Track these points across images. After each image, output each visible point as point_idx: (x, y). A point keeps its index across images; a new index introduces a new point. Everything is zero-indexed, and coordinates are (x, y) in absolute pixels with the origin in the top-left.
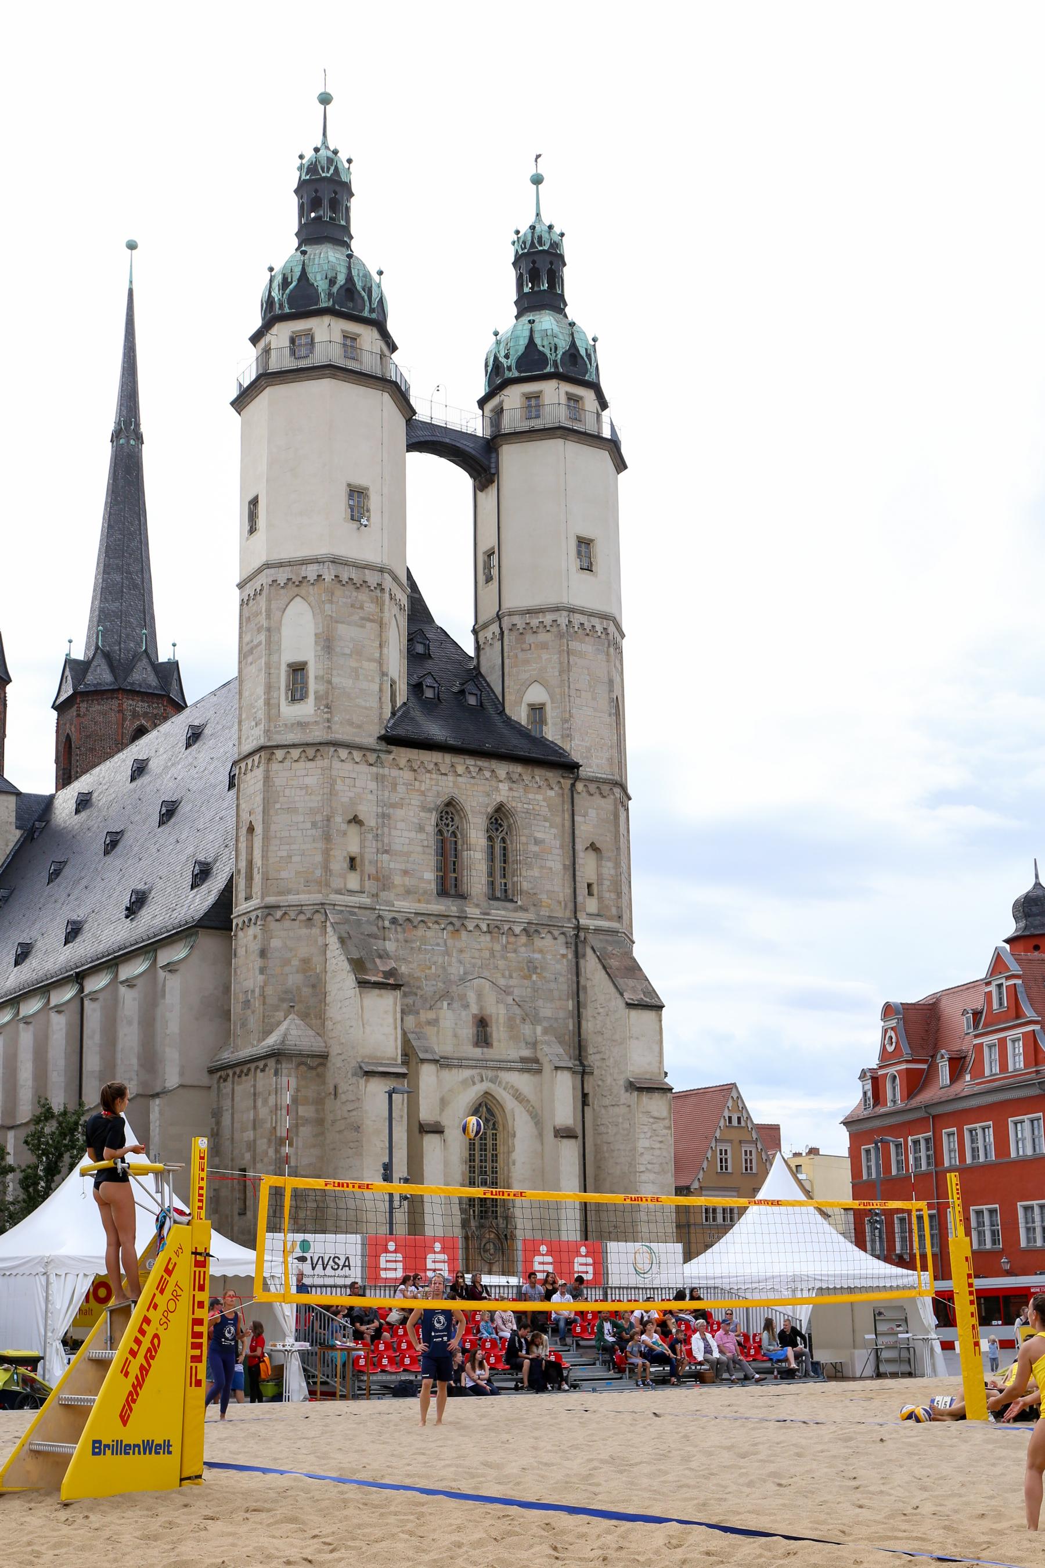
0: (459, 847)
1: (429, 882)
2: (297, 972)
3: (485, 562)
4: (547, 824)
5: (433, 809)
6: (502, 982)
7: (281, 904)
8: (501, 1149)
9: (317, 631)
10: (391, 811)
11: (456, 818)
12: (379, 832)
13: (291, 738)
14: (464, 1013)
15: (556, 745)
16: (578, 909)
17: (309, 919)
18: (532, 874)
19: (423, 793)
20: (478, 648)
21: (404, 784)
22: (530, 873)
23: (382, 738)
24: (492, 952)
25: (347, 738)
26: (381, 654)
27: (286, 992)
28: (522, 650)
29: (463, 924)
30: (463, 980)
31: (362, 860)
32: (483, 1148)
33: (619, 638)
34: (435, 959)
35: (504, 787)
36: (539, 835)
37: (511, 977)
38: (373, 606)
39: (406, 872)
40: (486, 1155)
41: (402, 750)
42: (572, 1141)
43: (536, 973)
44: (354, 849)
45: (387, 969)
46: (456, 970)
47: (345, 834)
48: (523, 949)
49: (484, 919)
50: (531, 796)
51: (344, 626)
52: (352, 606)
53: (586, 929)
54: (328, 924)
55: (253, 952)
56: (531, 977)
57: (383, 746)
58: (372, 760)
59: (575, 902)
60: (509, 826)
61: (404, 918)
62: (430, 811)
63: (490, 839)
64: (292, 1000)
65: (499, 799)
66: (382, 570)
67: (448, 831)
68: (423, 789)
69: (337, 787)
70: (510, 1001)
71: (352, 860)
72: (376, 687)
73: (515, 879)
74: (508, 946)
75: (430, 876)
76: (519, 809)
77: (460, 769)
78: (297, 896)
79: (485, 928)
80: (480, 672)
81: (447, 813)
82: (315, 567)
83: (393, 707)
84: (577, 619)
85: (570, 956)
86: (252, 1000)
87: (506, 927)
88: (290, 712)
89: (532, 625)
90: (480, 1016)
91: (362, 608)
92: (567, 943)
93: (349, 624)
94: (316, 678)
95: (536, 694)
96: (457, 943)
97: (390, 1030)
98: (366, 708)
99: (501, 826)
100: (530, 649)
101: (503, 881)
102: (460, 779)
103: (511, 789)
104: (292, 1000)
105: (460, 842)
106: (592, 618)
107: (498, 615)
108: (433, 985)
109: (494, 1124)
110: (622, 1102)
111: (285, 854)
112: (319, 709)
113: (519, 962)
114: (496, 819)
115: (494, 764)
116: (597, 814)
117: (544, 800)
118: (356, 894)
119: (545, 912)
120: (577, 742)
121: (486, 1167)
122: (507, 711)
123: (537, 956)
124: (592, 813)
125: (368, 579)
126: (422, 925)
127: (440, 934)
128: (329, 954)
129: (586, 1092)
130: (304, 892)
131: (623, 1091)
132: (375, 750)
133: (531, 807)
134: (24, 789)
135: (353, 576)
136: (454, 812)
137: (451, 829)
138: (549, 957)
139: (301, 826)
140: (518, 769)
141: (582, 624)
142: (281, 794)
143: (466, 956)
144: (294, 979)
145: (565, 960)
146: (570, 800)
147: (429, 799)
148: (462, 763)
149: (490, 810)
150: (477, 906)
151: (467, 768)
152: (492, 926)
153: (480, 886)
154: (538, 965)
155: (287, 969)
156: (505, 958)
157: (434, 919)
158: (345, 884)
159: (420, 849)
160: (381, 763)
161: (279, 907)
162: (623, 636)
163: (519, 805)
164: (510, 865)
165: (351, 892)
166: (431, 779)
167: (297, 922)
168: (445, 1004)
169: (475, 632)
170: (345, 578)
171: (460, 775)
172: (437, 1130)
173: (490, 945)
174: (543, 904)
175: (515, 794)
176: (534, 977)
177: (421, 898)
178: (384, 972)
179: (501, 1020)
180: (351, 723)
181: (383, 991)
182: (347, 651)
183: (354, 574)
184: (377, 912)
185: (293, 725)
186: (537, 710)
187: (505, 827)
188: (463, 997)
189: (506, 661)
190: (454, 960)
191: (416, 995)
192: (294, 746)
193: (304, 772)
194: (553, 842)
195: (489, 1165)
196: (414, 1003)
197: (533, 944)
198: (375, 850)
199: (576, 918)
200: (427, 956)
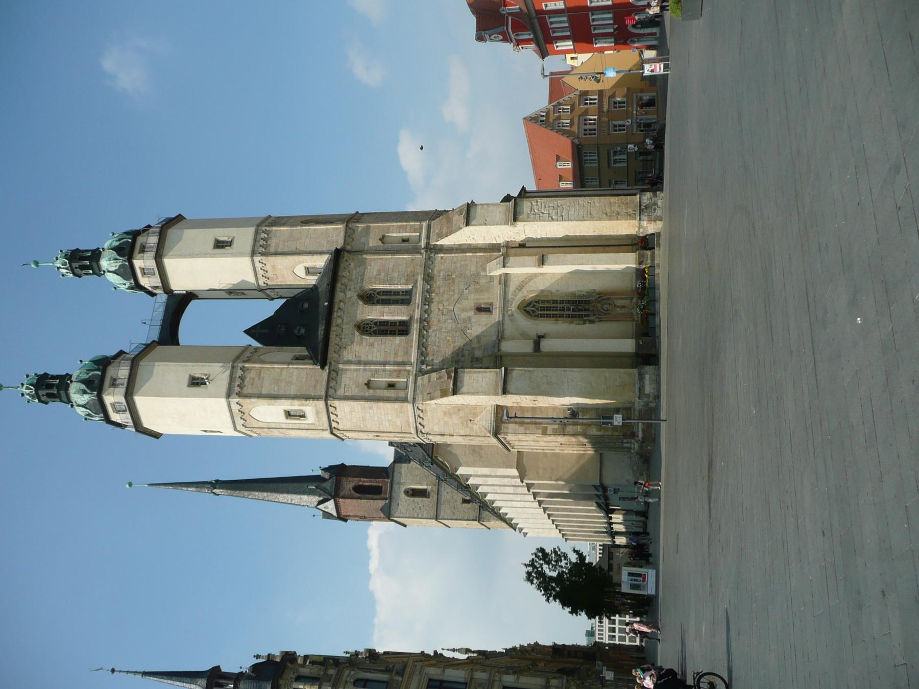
3: (234, 295)
5: (361, 337)
6: (456, 296)
7: (415, 426)
8: (550, 298)
14: (473, 320)
15: (326, 261)
17: (422, 412)
20: (281, 298)
23: (323, 367)
28: (277, 278)
30: (455, 320)
32: (549, 309)
33: (271, 219)
34: (443, 337)
36: (375, 272)
37: (454, 290)
39: (396, 354)
40: (553, 307)
41: (329, 356)
42: (544, 257)
43: (451, 276)
45: (446, 376)
46: (449, 325)
49: (421, 307)
50: (354, 278)
53: (428, 244)
56: (453, 278)
57: (327, 368)
62: (362, 339)
65: (356, 297)
67: (374, 327)
70: (466, 292)
72: (295, 370)
75: (397, 340)
78: (410, 418)
80: (294, 297)
88: (311, 418)
90: (475, 310)
91: (253, 379)
94: (292, 405)
95: (300, 271)
96: (435, 324)
97: (480, 375)
98: (307, 378)
99: (371, 294)
102: (345, 321)
104: (467, 422)
106: (257, 240)
107: (260, 291)
108: (458, 338)
109: (536, 302)
110: (523, 228)
113: (445, 285)
114: (367, 297)
115: (336, 300)
116: (364, 237)
121: (560, 307)
123: (442, 274)
129: (518, 245)
131: (515, 228)
132: (329, 373)
133: (359, 277)
134: (392, 460)
136: (363, 323)
137: (373, 325)
140: (339, 285)
144: (455, 419)
148: (336, 320)
150: (414, 311)
151: (339, 317)
154: (447, 274)
157: (421, 338)
159: (383, 346)
161: (416, 427)
162: (270, 216)
163: (359, 284)
166: (345, 339)
167: (424, 418)
168: (468, 331)
169: (272, 299)
171: (343, 321)
172: (538, 341)
175: (353, 287)
176: (454, 276)
178: (448, 378)
179: (477, 297)
181: (458, 380)
184: (417, 373)
185: (318, 418)
186: (308, 271)
187: (372, 292)
188: (465, 321)
191: (463, 349)
192: (329, 418)
193: (343, 412)
195: (559, 305)
196: (468, 350)
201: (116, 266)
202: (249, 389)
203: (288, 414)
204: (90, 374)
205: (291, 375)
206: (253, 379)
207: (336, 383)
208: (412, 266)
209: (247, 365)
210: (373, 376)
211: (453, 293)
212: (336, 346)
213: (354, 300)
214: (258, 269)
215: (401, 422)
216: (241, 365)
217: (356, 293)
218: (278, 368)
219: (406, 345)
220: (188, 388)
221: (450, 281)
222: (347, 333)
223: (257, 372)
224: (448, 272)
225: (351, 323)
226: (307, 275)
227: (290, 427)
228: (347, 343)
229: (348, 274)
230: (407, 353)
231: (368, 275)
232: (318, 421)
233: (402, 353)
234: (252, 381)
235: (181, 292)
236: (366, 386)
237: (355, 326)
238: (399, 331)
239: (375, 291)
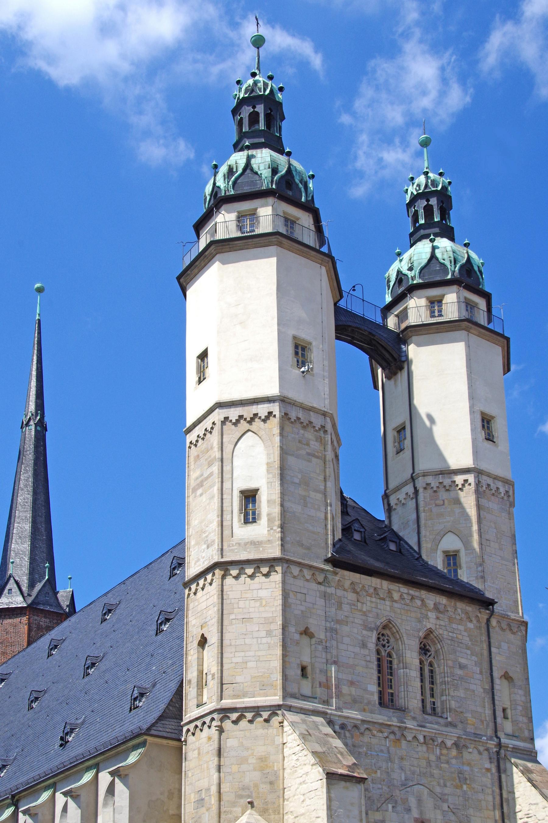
0: (395, 666)
1: (372, 694)
2: (255, 770)
4: (469, 652)
5: (374, 629)
9: (269, 461)
10: (338, 626)
11: (392, 640)
12: (328, 645)
15: (471, 585)
16: (498, 729)
18: (458, 695)
19: (365, 614)
21: (348, 604)
22: (456, 693)
23: (328, 561)
24: (429, 762)
26: (325, 487)
27: (244, 788)
29: (403, 734)
31: (313, 669)
35: (432, 615)
36: (463, 661)
38: (317, 444)
39: (352, 683)
41: (346, 573)
43: (466, 784)
44: (306, 659)
47: (297, 643)
48: (454, 761)
50: (454, 626)
52: (300, 442)
54: (286, 723)
55: (208, 752)
58: (320, 578)
59: (495, 723)
60: (436, 652)
61: (352, 725)
62: (371, 630)
63: (421, 662)
64: (249, 796)
66: (324, 414)
68: (364, 610)
69: (290, 600)
71: (303, 669)
72: (322, 516)
73: (444, 698)
74: (442, 757)
75: (374, 688)
76: (445, 637)
77: (396, 596)
79: (421, 739)
81: (383, 635)
83: (334, 539)
85: (494, 770)
86: (207, 798)
87: (440, 740)
89: (445, 484)
91: (308, 445)
92: (490, 758)
93: (298, 457)
94: (268, 501)
99: (429, 651)
100: (443, 505)
101: (433, 700)
102: (396, 605)
103: (438, 618)
105: (395, 662)
113: (452, 773)
114: (424, 645)
115: (424, 594)
117: (465, 630)
118: (310, 699)
119: (470, 729)
120: (489, 584)
122: (424, 557)
123: (466, 768)
125: (313, 420)
126: (367, 732)
127: (383, 742)
128: (287, 752)
130: (260, 695)
133: (455, 635)
135: (300, 416)
138: (476, 770)
139: (256, 635)
140: (443, 600)
143: (406, 763)
145: (489, 774)
146: (486, 633)
147: (370, 619)
149: (422, 634)
150: (414, 718)
152: (428, 738)
153: (416, 701)
154: (467, 777)
155: (244, 767)
156: (440, 768)
158: (299, 689)
159: (364, 663)
160: (329, 583)
163: (445, 633)
164: (439, 685)
165: (305, 698)
166: (371, 602)
170: (293, 415)
171: (396, 601)
173: (426, 755)
174: (469, 722)
175: (442, 623)
176: (465, 787)
177: (366, 707)
182: (297, 481)
185: (246, 544)
187: (433, 653)
189: (422, 515)
190: (396, 766)
197: (462, 757)
198: (325, 661)
199: (497, 737)
200: (373, 761)
211: (442, 784)
215: (242, 683)
217: (434, 628)
219: (365, 701)
220: (291, 335)
221: (457, 781)
222: (379, 607)
224: (470, 778)
227: (225, 496)
228: (365, 605)
230: (354, 703)
231: (459, 649)
232: (239, 544)
233: (353, 693)
236: (303, 629)
237: (390, 621)
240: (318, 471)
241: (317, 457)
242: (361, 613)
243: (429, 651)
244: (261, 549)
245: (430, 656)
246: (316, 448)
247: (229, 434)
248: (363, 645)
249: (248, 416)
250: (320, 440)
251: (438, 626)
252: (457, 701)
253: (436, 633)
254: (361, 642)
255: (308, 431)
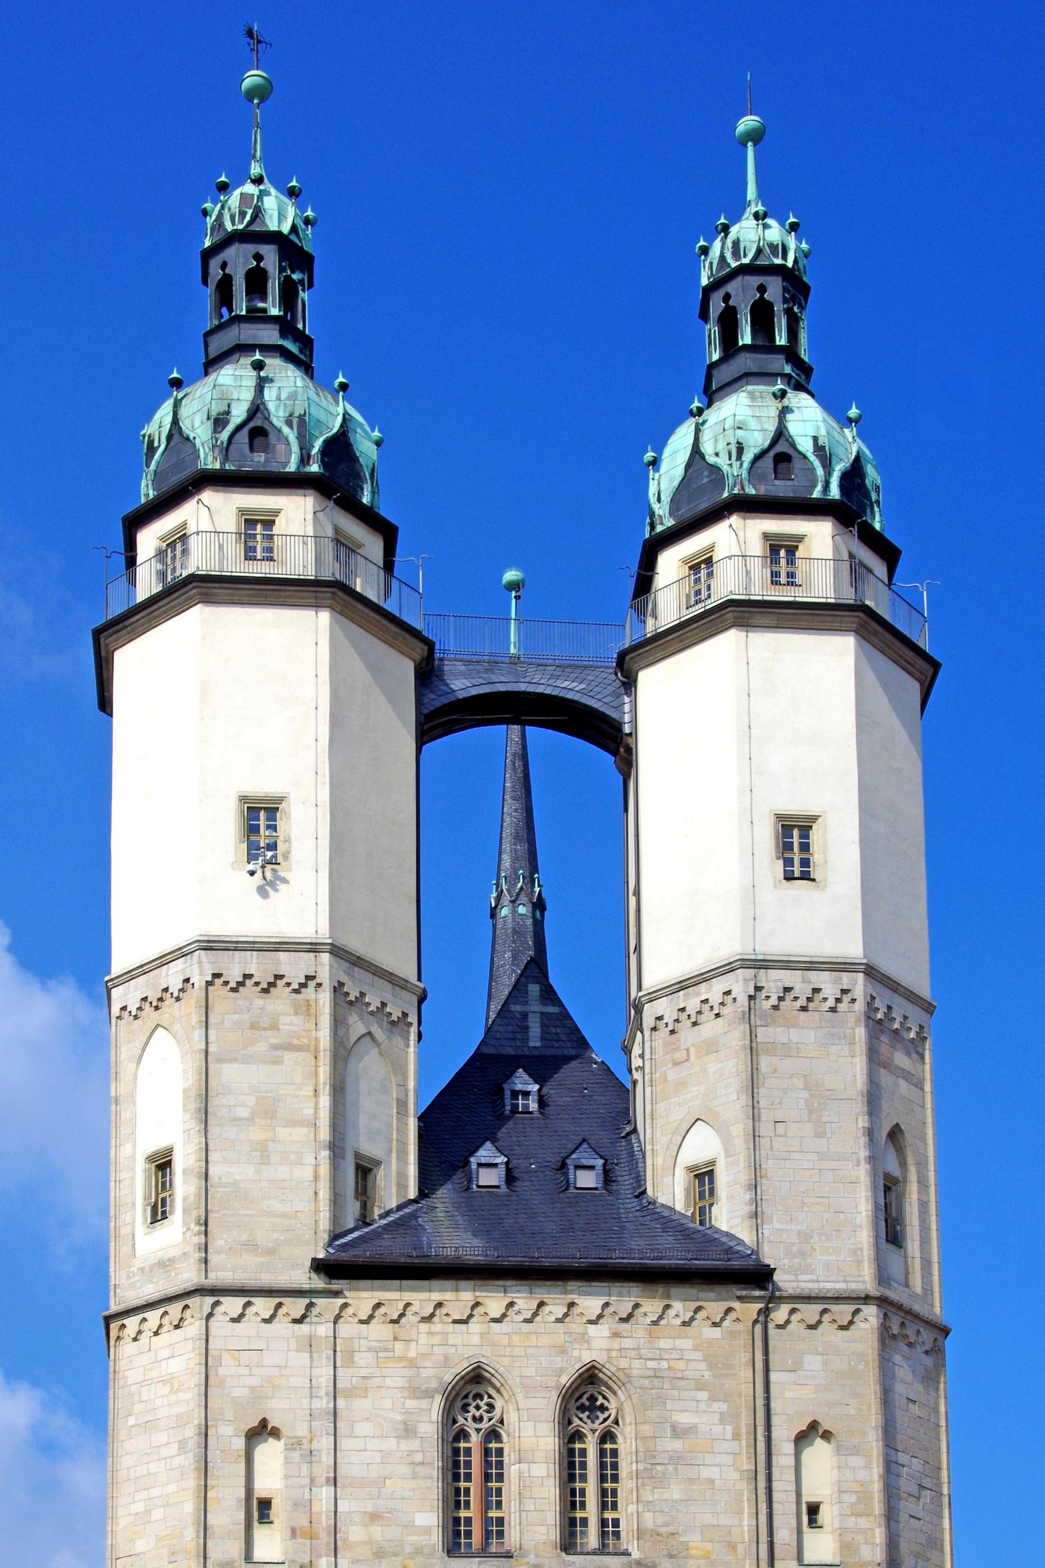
0: (506, 1459)
1: (426, 1531)
4: (703, 1395)
5: (436, 1391)
9: (187, 1085)
11: (499, 1404)
13: (150, 1291)
15: (733, 1237)
18: (666, 1496)
21: (369, 1349)
23: (319, 1266)
25: (245, 1276)
36: (684, 1419)
38: (298, 1020)
39: (374, 1517)
50: (663, 1343)
51: (236, 1066)
52: (253, 1026)
57: (319, 1282)
62: (429, 1394)
65: (587, 1357)
68: (412, 1354)
69: (222, 1371)
72: (308, 1173)
76: (635, 1372)
82: (177, 966)
84: (774, 980)
91: (274, 1027)
93: (246, 1061)
94: (185, 1172)
98: (284, 1215)
99: (603, 1408)
103: (616, 1335)
111: (139, 1507)
112: (188, 1229)
116: (825, 1363)
120: (777, 1225)
124: (813, 1363)
133: (664, 1364)
137: (484, 1425)
141: (787, 990)
142: (136, 1398)
147: (425, 1373)
149: (565, 1380)
159: (405, 1470)
163: (637, 1364)
166: (430, 1334)
174: (693, 1552)
175: (627, 1343)
180: (250, 1246)
182: (243, 1112)
183: (255, 964)
187: (613, 1412)
194: (718, 1429)
198: (307, 1481)
201: (717, 454)
202: (236, 1017)
203: (162, 1164)
204: (286, 430)
205: (293, 1157)
206: (274, 1027)
207: (265, 1321)
208: (709, 1546)
209: (325, 998)
210: (295, 1445)
212: (401, 1306)
213: (576, 1353)
214: (704, 991)
216: (324, 976)
217: (601, 1358)
218: (316, 1108)
219: (408, 1550)
223: (299, 1038)
225: (487, 1351)
226: (690, 1169)
228: (413, 1345)
229: (679, 1322)
231: (675, 1393)
234: (265, 1022)
235: (627, 718)
238: (468, 1521)
239: (617, 1423)
240: (298, 1079)
241: (298, 1048)
242: (403, 1365)
243: (603, 1408)
244: (173, 1274)
245: (605, 1420)
246: (295, 1028)
247: (129, 1042)
248: (407, 1431)
249: (153, 996)
250: (308, 1010)
251: (614, 1354)
252: (662, 1512)
253: (610, 1368)
254: (402, 1427)
255: (277, 998)
